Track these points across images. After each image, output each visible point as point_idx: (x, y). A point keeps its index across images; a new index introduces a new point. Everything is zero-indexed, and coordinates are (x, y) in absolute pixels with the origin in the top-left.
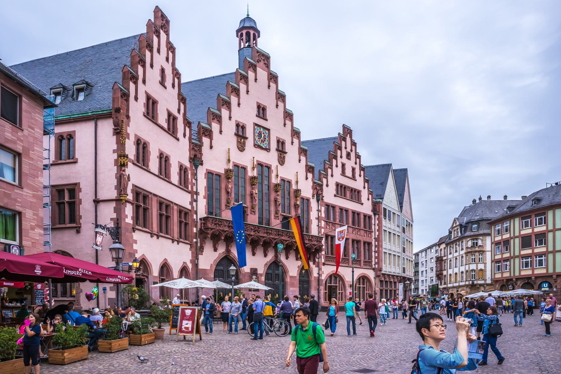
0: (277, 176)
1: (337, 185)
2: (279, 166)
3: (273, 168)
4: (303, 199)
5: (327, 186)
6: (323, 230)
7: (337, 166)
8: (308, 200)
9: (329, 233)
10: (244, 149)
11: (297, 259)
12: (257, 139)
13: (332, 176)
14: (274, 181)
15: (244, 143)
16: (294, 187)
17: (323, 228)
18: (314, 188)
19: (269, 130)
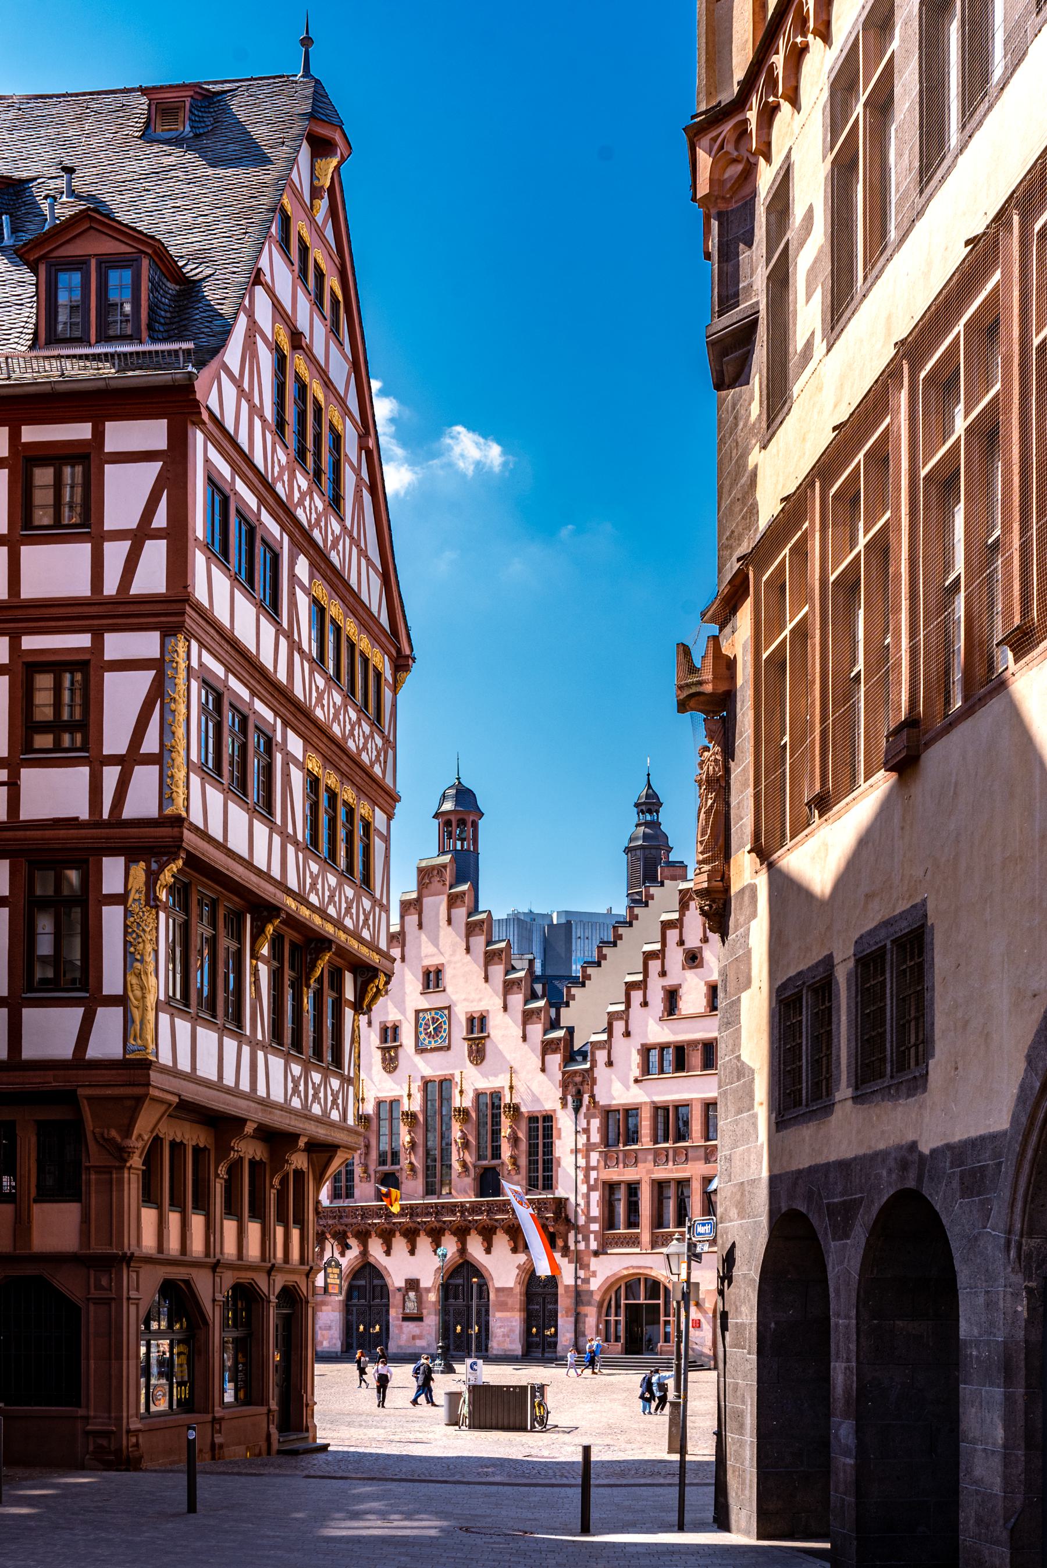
0: (461, 1092)
1: (645, 1051)
2: (470, 1070)
3: (457, 1079)
4: (533, 1119)
5: (610, 1063)
6: (593, 1174)
7: (645, 1004)
8: (548, 1118)
9: (616, 1178)
10: (395, 1068)
11: (515, 1250)
12: (422, 1036)
13: (627, 1034)
14: (457, 1102)
15: (396, 1057)
16: (507, 1100)
17: (594, 1168)
18: (565, 1085)
19: (449, 1008)
